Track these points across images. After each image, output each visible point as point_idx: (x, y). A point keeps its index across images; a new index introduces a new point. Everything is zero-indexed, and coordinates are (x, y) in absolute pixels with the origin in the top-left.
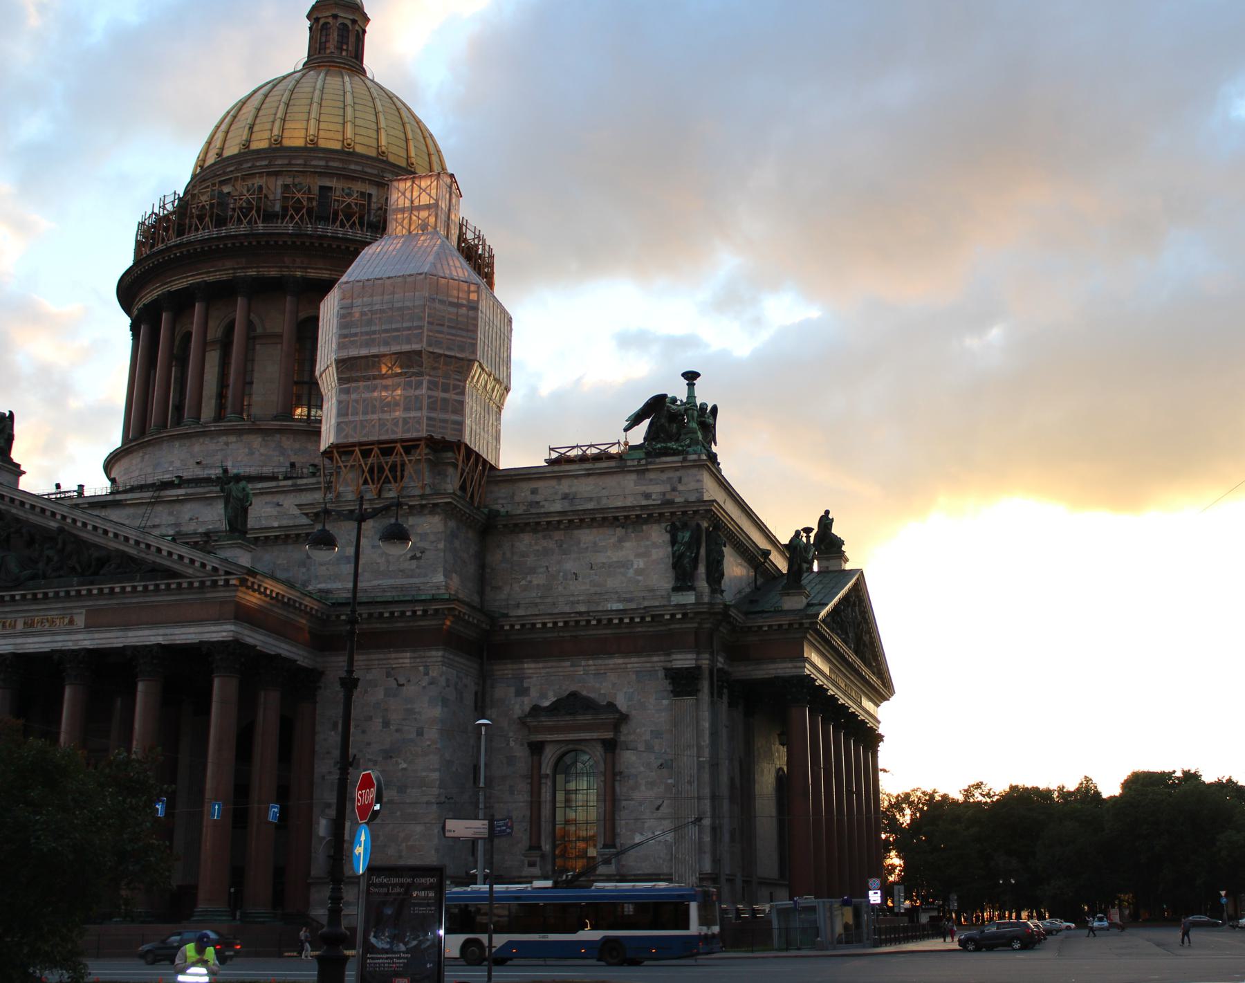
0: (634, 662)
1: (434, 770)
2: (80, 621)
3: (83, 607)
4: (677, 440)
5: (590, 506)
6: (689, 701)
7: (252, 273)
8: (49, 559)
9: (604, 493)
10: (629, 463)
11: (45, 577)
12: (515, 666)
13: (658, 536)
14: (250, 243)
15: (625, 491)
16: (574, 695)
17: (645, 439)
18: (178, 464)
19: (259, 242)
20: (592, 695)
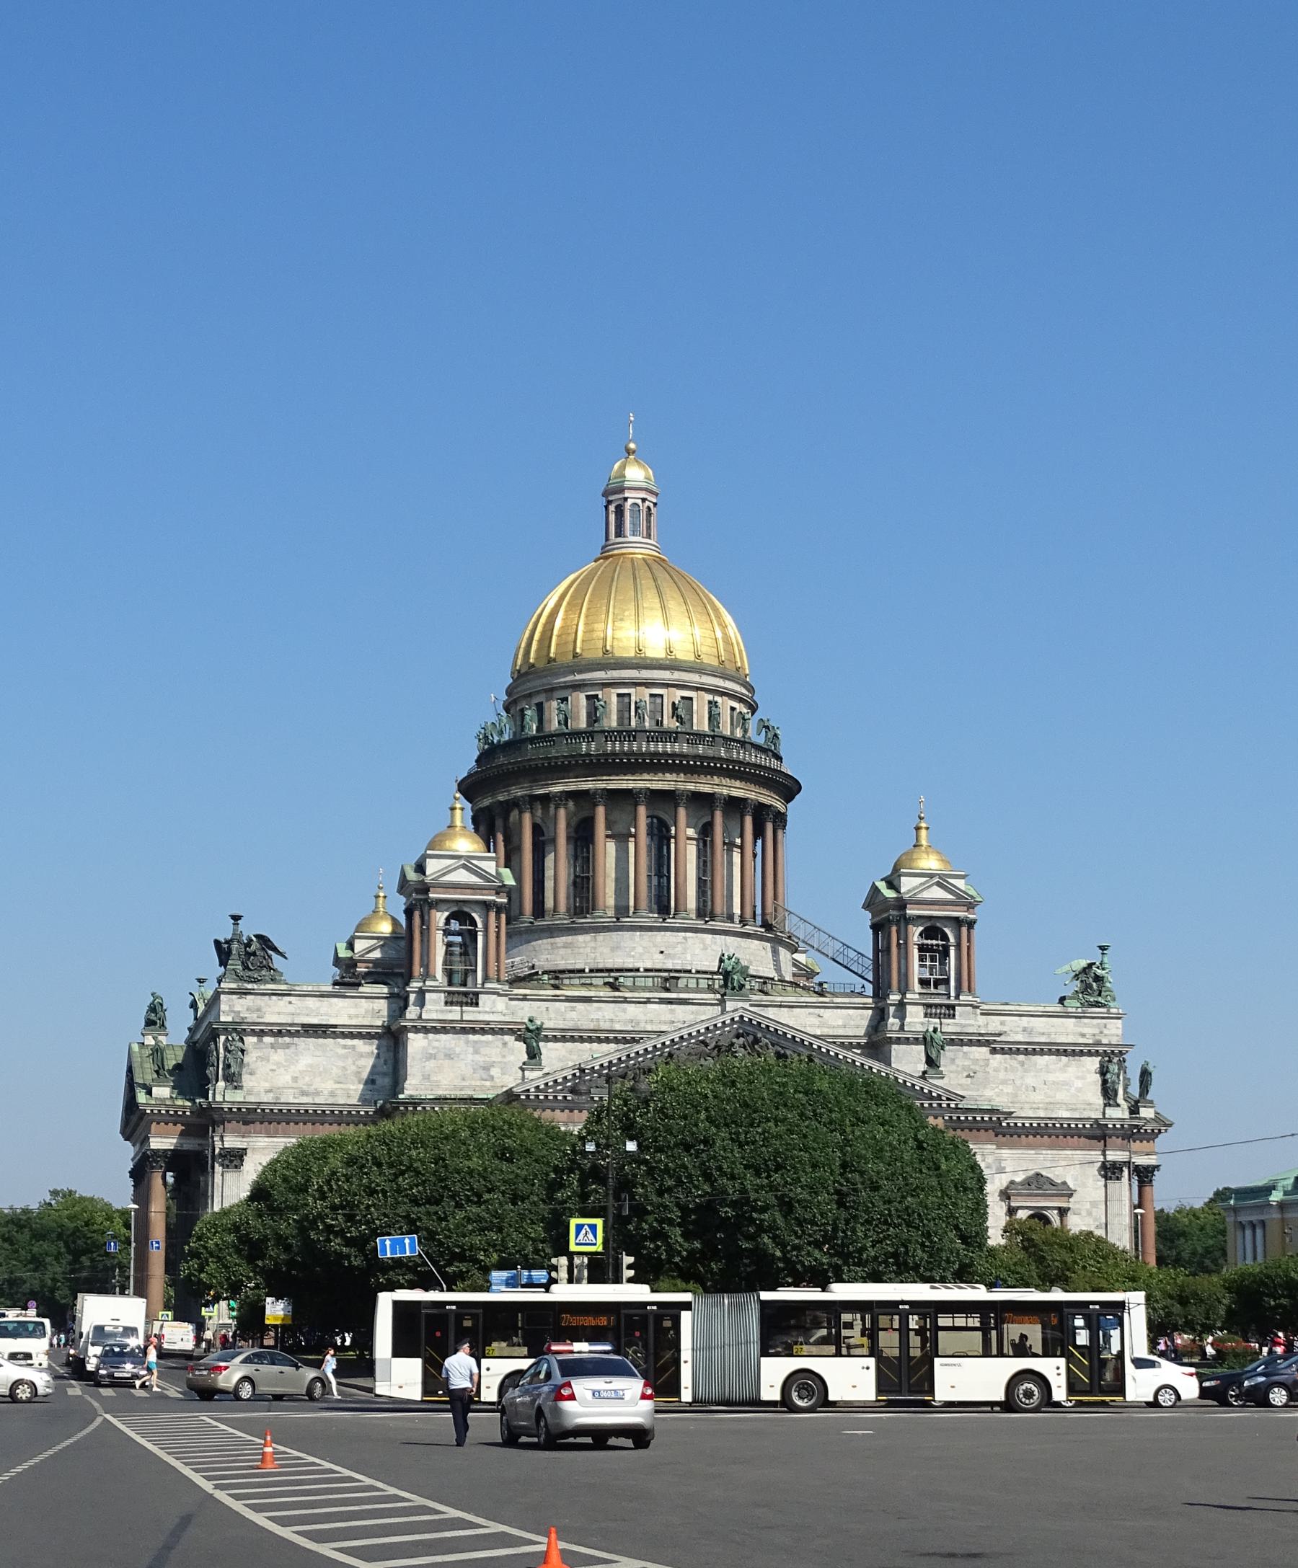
4: (1100, 995)
5: (1043, 1040)
7: (691, 787)
9: (1053, 1030)
10: (1070, 1010)
13: (1093, 1063)
15: (1068, 1031)
18: (640, 950)
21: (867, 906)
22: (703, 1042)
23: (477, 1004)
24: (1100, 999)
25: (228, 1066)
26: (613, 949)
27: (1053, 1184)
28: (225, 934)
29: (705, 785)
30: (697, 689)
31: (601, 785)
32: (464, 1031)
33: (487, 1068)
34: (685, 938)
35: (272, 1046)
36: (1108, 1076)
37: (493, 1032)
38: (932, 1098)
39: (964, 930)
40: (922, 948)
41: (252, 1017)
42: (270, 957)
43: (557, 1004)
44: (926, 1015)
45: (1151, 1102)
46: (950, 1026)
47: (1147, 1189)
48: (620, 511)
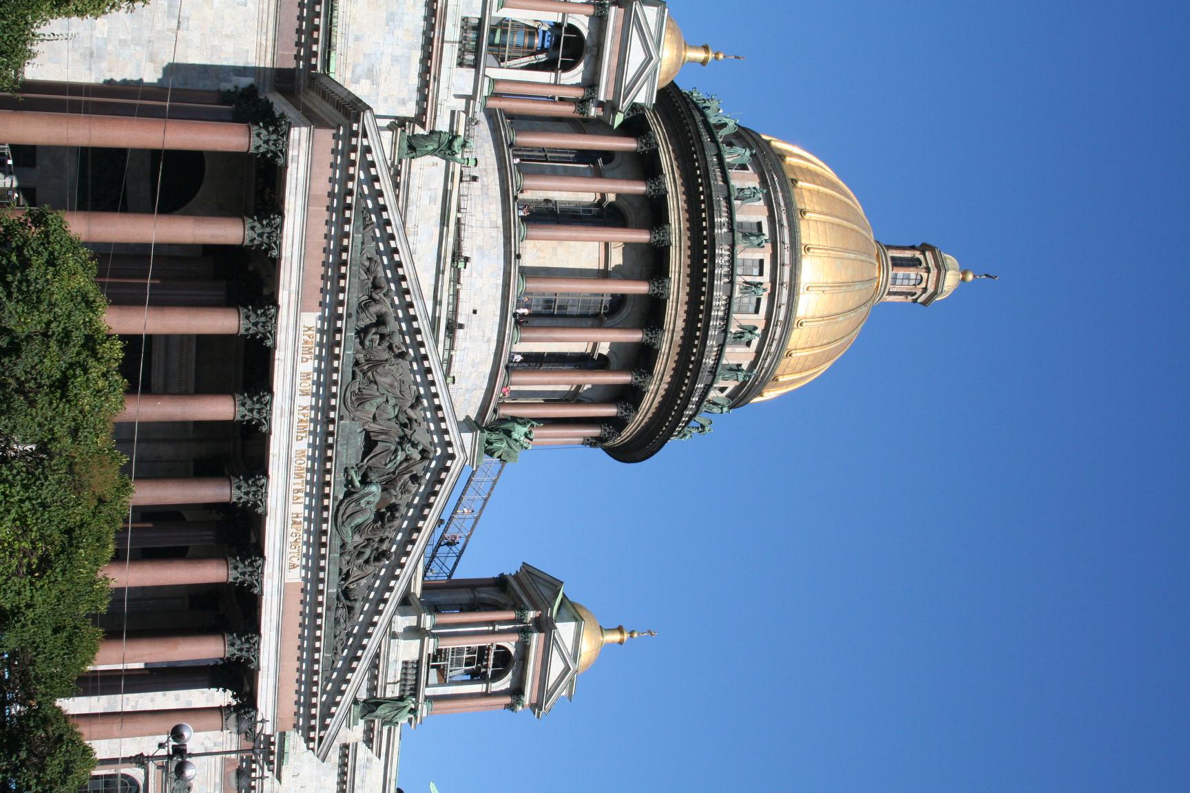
7: (665, 348)
8: (360, 554)
11: (341, 554)
21: (527, 569)
22: (418, 398)
23: (461, 64)
26: (480, 249)
29: (664, 366)
31: (674, 239)
32: (428, 42)
33: (371, 74)
34: (489, 341)
37: (424, 84)
38: (323, 719)
39: (508, 700)
40: (483, 651)
44: (406, 663)
48: (914, 263)
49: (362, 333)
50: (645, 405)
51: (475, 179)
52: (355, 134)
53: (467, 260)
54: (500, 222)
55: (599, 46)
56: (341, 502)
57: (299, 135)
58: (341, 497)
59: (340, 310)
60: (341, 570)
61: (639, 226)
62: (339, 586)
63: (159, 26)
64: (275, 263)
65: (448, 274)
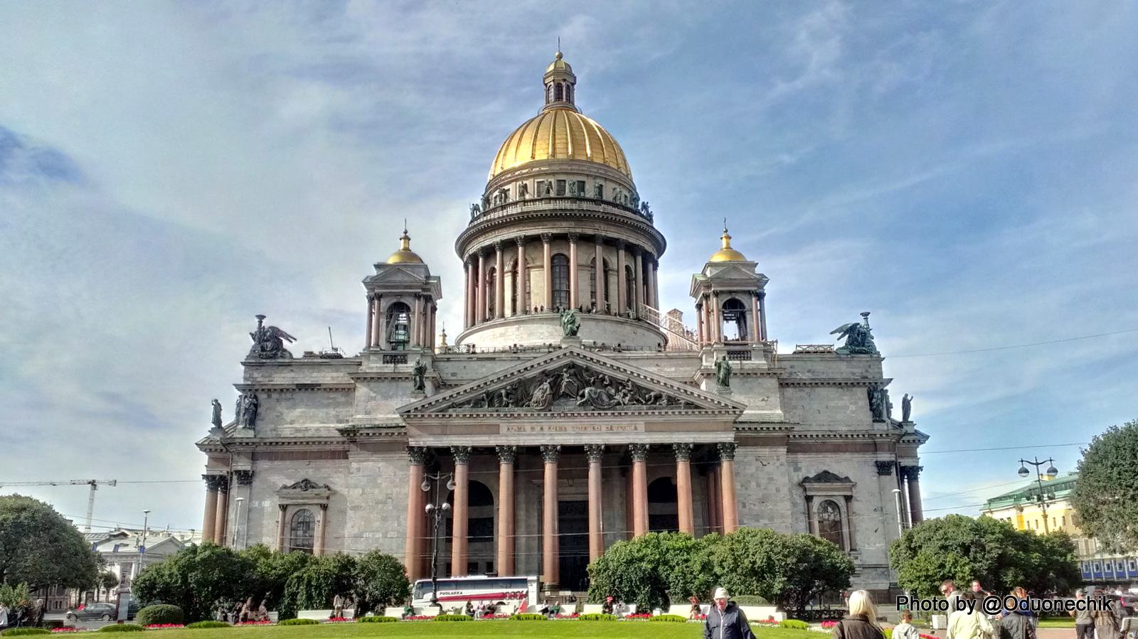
0: (857, 457)
1: (787, 510)
2: (641, 427)
3: (642, 421)
4: (863, 346)
5: (824, 376)
6: (888, 477)
7: (579, 230)
12: (793, 456)
13: (862, 393)
14: (580, 215)
15: (843, 370)
16: (826, 472)
17: (846, 344)
19: (585, 215)
20: (835, 473)
24: (864, 348)
25: (244, 414)
27: (836, 478)
28: (255, 329)
30: (588, 175)
31: (522, 234)
35: (278, 400)
36: (874, 400)
41: (266, 381)
42: (282, 341)
43: (472, 363)
45: (912, 422)
46: (749, 364)
47: (914, 483)
49: (507, 405)
50: (615, 235)
51: (474, 346)
52: (409, 416)
53: (515, 345)
54: (517, 326)
55: (396, 295)
56: (595, 407)
57: (412, 443)
58: (592, 407)
59: (495, 415)
60: (634, 404)
61: (517, 253)
62: (642, 403)
63: (391, 508)
64: (476, 450)
65: (521, 355)
